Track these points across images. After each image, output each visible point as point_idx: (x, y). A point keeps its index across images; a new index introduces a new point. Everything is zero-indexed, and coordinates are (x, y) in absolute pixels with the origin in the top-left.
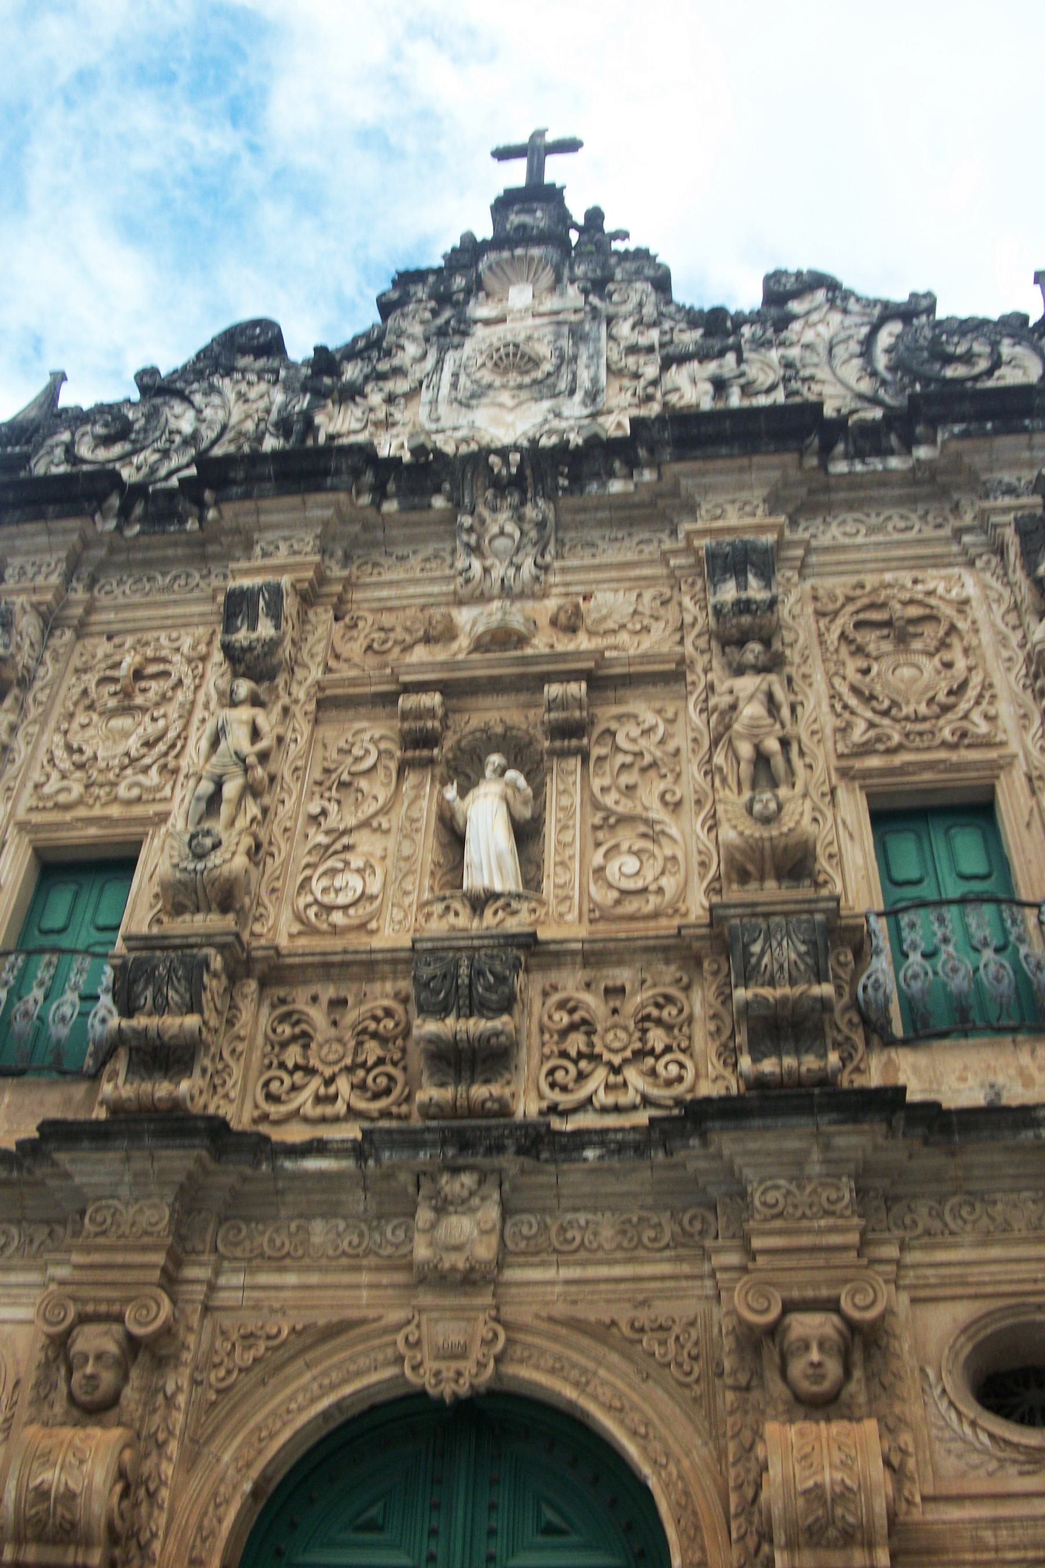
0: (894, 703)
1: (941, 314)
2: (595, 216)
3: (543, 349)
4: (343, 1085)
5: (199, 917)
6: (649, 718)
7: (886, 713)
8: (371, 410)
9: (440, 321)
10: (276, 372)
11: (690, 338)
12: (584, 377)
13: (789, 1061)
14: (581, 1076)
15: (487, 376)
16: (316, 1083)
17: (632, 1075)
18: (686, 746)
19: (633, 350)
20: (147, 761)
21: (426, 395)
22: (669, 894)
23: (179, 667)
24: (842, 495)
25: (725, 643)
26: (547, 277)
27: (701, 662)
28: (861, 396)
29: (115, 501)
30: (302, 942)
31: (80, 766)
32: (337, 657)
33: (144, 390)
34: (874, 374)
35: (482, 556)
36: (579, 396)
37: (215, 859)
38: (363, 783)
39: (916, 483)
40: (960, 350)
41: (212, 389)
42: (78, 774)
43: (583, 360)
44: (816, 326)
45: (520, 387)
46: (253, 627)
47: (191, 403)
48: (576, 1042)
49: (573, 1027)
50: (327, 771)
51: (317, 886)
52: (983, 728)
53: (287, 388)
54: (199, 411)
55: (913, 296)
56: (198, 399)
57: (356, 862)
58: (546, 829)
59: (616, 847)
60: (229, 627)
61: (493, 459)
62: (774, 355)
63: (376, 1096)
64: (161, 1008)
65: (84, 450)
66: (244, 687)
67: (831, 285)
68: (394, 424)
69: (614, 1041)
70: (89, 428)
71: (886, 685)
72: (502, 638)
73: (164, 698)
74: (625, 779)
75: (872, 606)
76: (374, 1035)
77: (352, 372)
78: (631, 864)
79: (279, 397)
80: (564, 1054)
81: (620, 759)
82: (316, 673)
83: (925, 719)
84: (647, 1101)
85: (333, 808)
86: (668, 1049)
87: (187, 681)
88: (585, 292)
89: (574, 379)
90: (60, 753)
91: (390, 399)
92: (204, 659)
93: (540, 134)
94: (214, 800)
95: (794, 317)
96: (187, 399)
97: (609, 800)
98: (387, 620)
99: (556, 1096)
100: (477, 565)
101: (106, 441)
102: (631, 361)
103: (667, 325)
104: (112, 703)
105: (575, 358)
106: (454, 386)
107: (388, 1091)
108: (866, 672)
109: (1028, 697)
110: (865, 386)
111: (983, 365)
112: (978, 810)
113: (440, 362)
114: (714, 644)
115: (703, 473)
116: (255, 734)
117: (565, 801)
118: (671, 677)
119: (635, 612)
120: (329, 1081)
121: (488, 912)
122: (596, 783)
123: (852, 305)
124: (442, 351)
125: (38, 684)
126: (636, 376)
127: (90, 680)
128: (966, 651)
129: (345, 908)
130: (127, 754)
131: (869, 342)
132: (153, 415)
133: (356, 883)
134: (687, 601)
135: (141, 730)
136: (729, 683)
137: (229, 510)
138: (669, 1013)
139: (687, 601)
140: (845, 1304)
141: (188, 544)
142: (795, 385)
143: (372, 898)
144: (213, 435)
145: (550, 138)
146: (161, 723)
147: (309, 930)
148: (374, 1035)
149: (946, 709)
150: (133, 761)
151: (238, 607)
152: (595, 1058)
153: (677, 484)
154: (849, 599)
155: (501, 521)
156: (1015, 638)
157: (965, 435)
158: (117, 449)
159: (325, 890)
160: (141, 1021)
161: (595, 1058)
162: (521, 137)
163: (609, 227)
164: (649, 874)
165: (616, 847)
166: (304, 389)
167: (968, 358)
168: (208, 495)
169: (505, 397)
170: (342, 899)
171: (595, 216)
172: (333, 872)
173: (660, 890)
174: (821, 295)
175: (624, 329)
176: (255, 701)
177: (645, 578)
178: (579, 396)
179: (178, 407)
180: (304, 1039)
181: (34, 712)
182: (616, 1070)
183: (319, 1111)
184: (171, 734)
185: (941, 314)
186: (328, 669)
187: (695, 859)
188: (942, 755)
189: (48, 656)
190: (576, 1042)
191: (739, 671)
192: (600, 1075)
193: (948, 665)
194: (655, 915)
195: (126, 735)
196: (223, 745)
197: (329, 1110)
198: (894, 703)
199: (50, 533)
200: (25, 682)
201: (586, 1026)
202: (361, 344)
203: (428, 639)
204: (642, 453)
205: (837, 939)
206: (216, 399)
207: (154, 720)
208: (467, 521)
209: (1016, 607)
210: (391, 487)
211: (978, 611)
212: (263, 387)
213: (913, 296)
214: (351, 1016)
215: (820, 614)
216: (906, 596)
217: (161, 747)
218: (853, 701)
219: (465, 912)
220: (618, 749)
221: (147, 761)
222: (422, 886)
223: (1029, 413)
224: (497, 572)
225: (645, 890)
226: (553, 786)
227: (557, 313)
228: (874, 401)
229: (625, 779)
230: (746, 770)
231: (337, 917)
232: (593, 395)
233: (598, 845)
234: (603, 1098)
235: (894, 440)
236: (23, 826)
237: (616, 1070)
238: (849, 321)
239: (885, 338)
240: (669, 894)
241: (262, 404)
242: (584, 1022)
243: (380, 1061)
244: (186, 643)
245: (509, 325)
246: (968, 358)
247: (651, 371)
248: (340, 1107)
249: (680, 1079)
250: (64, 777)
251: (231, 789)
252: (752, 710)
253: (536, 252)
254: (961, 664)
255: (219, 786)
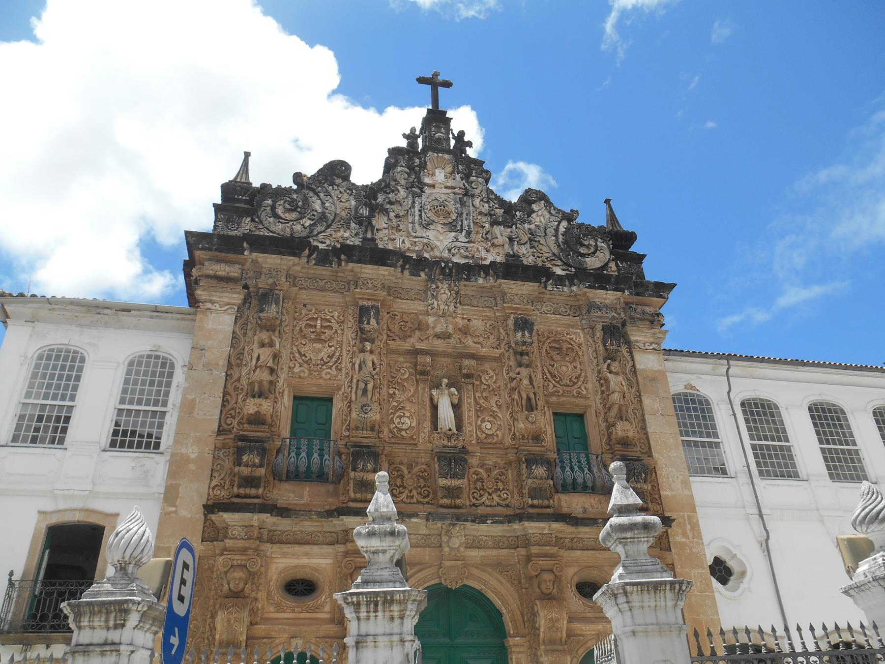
0: (561, 379)
1: (579, 220)
2: (462, 134)
3: (451, 207)
4: (414, 492)
5: (365, 432)
6: (491, 373)
7: (558, 382)
8: (390, 220)
9: (411, 180)
10: (351, 190)
11: (500, 212)
12: (465, 223)
13: (541, 501)
14: (481, 496)
15: (434, 218)
16: (406, 491)
17: (494, 496)
18: (502, 387)
19: (481, 213)
20: (330, 364)
21: (410, 219)
22: (500, 437)
23: (335, 326)
24: (548, 296)
25: (516, 353)
26: (449, 169)
27: (507, 354)
28: (554, 254)
29: (307, 251)
30: (393, 440)
31: (306, 362)
32: (390, 330)
33: (295, 182)
34: (559, 246)
35: (437, 300)
36: (464, 233)
37: (370, 414)
38: (405, 384)
39: (570, 296)
40: (586, 243)
41: (328, 194)
42: (306, 366)
43: (464, 215)
44: (540, 216)
45: (444, 224)
46: (368, 323)
47: (318, 196)
48: (479, 485)
49: (478, 480)
50: (393, 377)
51: (396, 421)
52: (585, 393)
53: (356, 200)
54: (323, 203)
55: (572, 211)
56: (322, 195)
57: (407, 414)
58: (463, 408)
59: (484, 418)
60: (361, 322)
61: (443, 265)
62: (526, 226)
63: (424, 497)
64: (364, 470)
65: (280, 211)
66: (368, 346)
67: (547, 201)
68: (400, 230)
69: (489, 485)
70: (282, 202)
71: (558, 371)
72: (444, 336)
73: (331, 339)
74: (485, 394)
75: (555, 341)
76: (422, 477)
77: (380, 198)
78: (489, 426)
79: (353, 203)
80: (476, 488)
81: (483, 386)
82: (385, 337)
83: (569, 386)
84: (498, 504)
85: (397, 392)
86: (503, 489)
87: (339, 332)
88: (462, 179)
89: (462, 225)
90: (297, 355)
91: (397, 216)
92: (342, 322)
93: (436, 75)
94: (365, 391)
95: (534, 212)
96: (316, 194)
97: (481, 401)
98: (405, 318)
99: (474, 501)
100: (435, 302)
101: (290, 211)
102: (479, 217)
103: (492, 204)
104: (313, 336)
105: (462, 214)
106: (420, 216)
107: (428, 496)
108: (553, 366)
109: (597, 384)
110: (556, 251)
111: (592, 250)
112: (581, 417)
113: (414, 202)
114: (511, 351)
115: (509, 284)
116: (373, 364)
117: (469, 401)
118: (498, 359)
119: (485, 330)
120: (410, 491)
121: (453, 440)
122: (477, 394)
123: (553, 212)
124: (415, 195)
125: (284, 324)
126: (483, 227)
127: (302, 324)
128: (580, 363)
129: (405, 430)
130: (322, 359)
131: (557, 230)
132: (306, 200)
133: (408, 421)
134: (502, 331)
135: (325, 350)
136: (518, 370)
137: (351, 265)
138: (503, 477)
139: (502, 331)
140: (555, 570)
141: (331, 271)
142: (535, 244)
143: (414, 427)
144: (332, 218)
145: (440, 78)
146: (333, 348)
147: (395, 436)
148: (422, 477)
149: (575, 384)
150: (325, 363)
151: (364, 312)
152: (484, 490)
153: (500, 284)
154: (548, 337)
155: (444, 287)
156: (595, 362)
157: (590, 287)
158: (294, 215)
159: (398, 423)
160: (359, 475)
161: (484, 490)
162: (429, 75)
163: (466, 139)
164: (494, 429)
165: (484, 418)
166: (366, 205)
167: (588, 247)
168: (343, 257)
169: (439, 227)
170: (404, 427)
171: (462, 134)
172: (400, 417)
173: (497, 435)
174: (543, 202)
175: (477, 201)
176: (371, 352)
177: (487, 316)
178: (464, 233)
179: (314, 199)
180: (402, 477)
181: (285, 336)
182: (490, 495)
183: (409, 501)
184: (337, 354)
185: (579, 220)
186: (388, 336)
187: (507, 427)
188: (573, 399)
189: (284, 310)
190: (479, 485)
191: (520, 365)
192: (486, 495)
193: (575, 367)
194: (496, 443)
195: (320, 351)
196: (364, 369)
197: (412, 501)
198: (561, 379)
199: (281, 259)
200: (280, 325)
201: (481, 480)
202: (383, 184)
203: (419, 329)
204: (491, 272)
205: (549, 464)
206: (331, 200)
207: (330, 347)
208: (434, 286)
209: (596, 351)
210: (407, 266)
211: (584, 349)
212: (345, 196)
213: (572, 211)
214: (415, 470)
215: (539, 341)
216: (564, 338)
217: (334, 359)
218: (549, 377)
219: (446, 439)
220: (482, 383)
221: (330, 364)
222: (427, 425)
223: (609, 283)
224: (442, 307)
225: (493, 435)
226: (465, 394)
227: (454, 188)
228: (561, 260)
229: (485, 394)
230: (524, 402)
231: (403, 433)
232: (469, 233)
233: (478, 417)
234: (487, 503)
235: (567, 283)
236: (289, 385)
237: (490, 495)
238: (553, 218)
239: (562, 229)
240: (500, 437)
241: (346, 205)
242: (481, 478)
243: (425, 486)
244: (336, 314)
245: (436, 190)
246: (588, 247)
247: (487, 225)
248: (415, 500)
249: (507, 498)
250: (301, 366)
251: (370, 386)
252: (526, 382)
253: (446, 156)
254: (578, 367)
255: (366, 385)
